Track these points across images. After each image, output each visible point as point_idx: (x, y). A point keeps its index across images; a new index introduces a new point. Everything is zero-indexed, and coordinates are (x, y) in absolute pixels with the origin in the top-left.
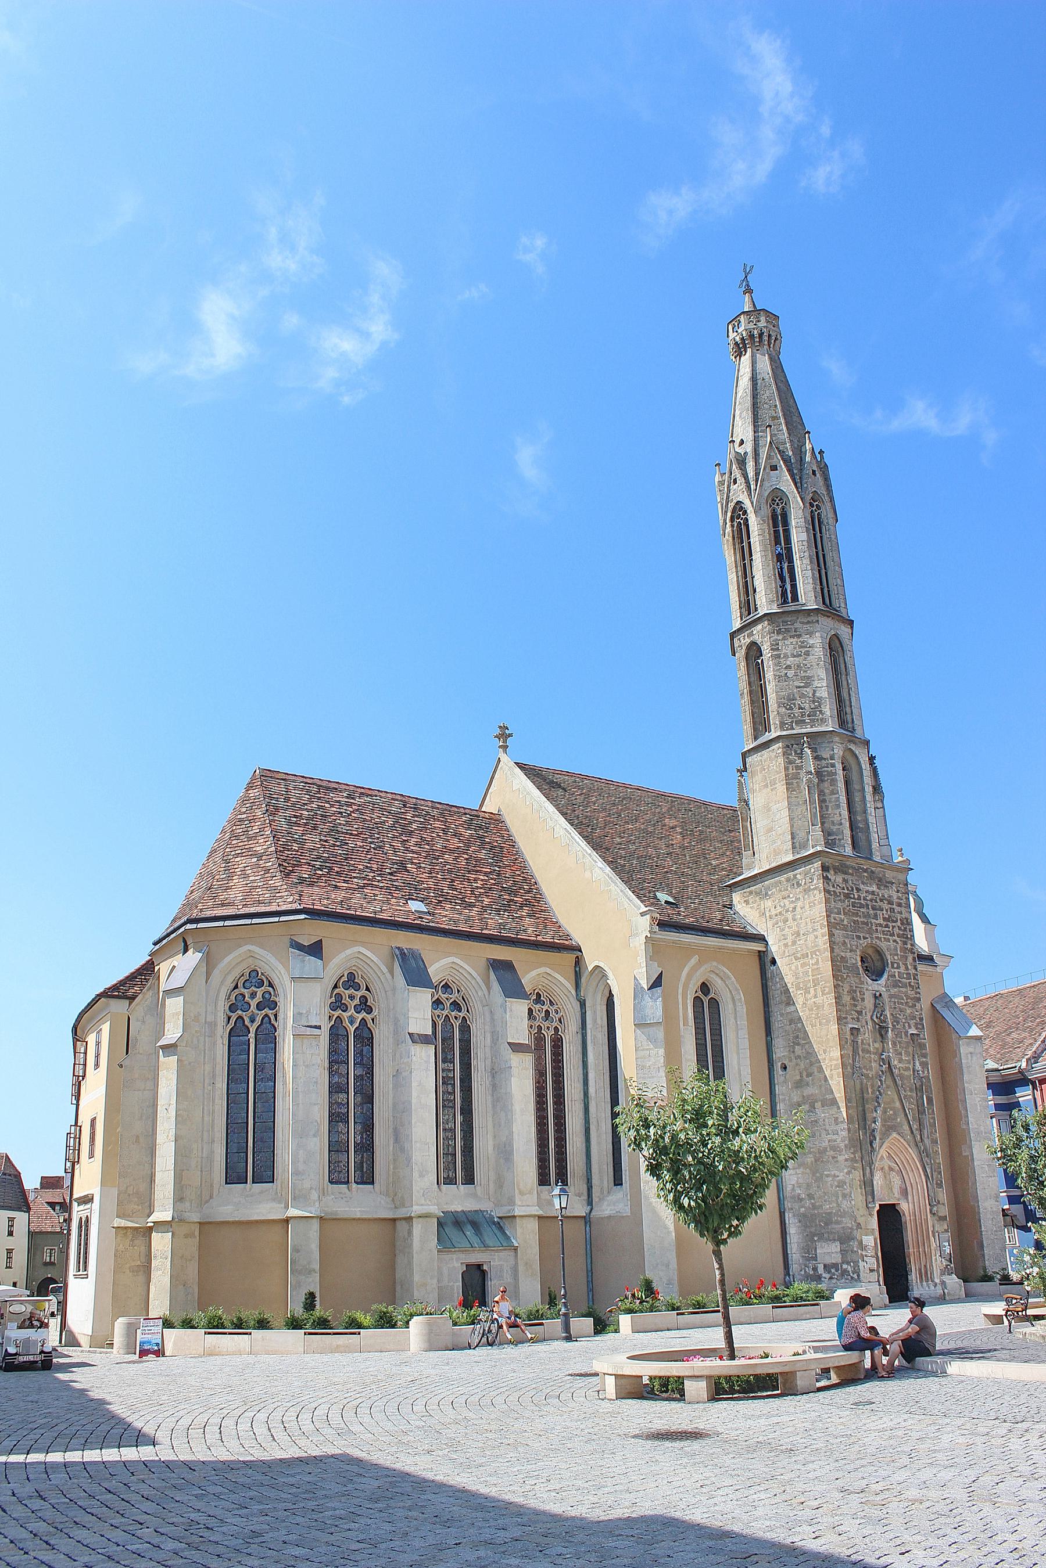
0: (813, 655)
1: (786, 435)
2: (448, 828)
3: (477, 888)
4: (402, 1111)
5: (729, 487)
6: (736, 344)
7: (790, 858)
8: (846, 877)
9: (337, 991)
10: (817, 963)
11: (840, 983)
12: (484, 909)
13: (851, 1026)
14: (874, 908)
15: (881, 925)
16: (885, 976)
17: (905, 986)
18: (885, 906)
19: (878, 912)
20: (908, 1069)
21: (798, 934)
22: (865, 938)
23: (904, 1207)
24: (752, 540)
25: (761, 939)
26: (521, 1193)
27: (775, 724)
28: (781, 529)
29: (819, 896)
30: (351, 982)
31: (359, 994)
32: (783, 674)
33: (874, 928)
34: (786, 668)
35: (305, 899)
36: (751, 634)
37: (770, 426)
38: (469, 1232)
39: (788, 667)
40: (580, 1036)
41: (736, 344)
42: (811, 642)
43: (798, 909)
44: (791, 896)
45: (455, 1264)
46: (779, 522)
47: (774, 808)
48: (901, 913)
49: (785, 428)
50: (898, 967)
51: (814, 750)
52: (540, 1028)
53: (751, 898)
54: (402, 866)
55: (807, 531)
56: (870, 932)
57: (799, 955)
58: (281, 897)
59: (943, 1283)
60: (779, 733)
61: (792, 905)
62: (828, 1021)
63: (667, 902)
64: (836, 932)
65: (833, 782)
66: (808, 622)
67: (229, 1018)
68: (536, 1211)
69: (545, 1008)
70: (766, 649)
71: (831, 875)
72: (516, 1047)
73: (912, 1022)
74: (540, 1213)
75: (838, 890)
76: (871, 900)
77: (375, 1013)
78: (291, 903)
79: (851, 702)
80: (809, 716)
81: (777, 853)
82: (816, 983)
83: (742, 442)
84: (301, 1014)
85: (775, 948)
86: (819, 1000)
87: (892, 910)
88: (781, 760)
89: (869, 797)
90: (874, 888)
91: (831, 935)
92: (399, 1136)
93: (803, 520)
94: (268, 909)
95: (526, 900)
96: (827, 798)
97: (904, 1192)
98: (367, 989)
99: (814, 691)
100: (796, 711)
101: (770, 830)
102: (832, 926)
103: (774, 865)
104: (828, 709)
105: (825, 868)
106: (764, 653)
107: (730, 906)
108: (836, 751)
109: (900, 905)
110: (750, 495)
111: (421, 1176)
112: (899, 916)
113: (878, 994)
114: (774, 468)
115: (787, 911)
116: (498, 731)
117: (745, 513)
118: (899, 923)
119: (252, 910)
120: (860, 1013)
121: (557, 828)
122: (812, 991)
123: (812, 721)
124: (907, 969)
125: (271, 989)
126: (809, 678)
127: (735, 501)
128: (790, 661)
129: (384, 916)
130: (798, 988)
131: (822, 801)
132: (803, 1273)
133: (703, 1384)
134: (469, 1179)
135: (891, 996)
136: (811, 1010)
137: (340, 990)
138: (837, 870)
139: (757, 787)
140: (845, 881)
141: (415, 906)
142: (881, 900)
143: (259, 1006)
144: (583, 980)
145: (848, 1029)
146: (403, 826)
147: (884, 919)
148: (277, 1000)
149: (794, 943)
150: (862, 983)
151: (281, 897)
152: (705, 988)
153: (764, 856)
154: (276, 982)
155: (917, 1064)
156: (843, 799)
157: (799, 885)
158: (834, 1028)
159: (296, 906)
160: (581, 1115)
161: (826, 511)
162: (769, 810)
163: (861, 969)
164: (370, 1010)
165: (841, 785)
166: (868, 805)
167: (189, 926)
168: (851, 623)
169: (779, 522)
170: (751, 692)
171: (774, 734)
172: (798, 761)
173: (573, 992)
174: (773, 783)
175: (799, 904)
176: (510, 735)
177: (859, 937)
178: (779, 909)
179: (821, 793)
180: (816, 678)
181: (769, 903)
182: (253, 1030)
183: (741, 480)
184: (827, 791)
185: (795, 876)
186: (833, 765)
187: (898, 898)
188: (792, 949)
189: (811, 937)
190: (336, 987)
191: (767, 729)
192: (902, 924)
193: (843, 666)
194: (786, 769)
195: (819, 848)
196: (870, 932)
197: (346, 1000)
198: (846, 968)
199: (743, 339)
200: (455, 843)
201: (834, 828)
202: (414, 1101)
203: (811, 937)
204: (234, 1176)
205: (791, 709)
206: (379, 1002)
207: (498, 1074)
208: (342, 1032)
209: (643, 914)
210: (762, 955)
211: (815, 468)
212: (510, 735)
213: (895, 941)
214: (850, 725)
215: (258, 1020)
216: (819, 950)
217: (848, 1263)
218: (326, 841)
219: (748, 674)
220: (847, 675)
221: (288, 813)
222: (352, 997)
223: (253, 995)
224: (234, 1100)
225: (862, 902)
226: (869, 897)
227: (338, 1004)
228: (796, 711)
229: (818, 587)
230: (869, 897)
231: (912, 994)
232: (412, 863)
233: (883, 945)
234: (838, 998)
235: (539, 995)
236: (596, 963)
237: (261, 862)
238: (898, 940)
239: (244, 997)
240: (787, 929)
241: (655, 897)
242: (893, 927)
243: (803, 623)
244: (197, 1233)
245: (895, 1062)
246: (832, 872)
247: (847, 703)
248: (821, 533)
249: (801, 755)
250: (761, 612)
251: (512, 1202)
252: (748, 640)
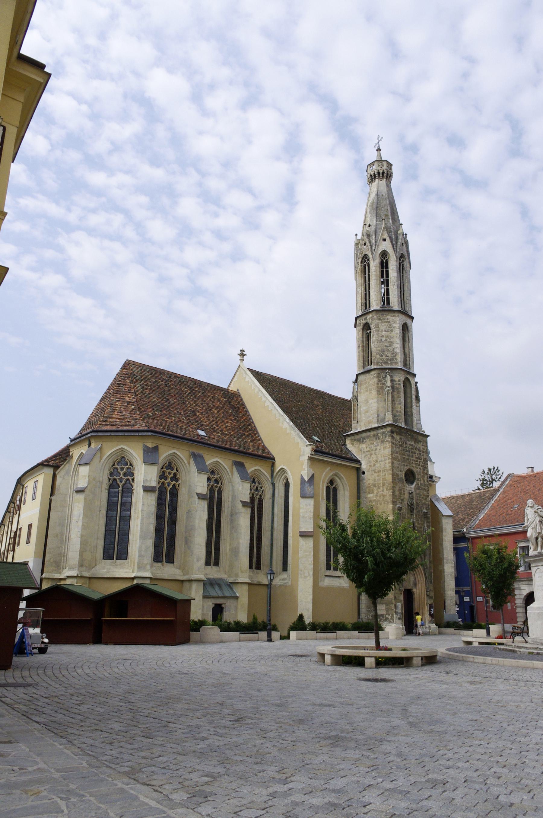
0: (395, 332)
1: (391, 224)
2: (215, 397)
3: (228, 426)
4: (189, 530)
5: (361, 246)
6: (371, 176)
7: (375, 425)
8: (401, 437)
9: (163, 470)
10: (385, 475)
11: (395, 486)
12: (231, 436)
13: (398, 506)
14: (412, 452)
15: (414, 460)
16: (415, 484)
17: (423, 489)
18: (417, 452)
19: (414, 454)
20: (421, 528)
21: (377, 461)
22: (407, 466)
23: (414, 590)
24: (371, 274)
25: (358, 462)
26: (242, 572)
27: (374, 362)
28: (385, 270)
29: (388, 445)
30: (169, 465)
31: (173, 472)
32: (380, 339)
33: (411, 462)
34: (381, 337)
35: (151, 426)
36: (366, 319)
37: (384, 219)
38: (217, 588)
39: (383, 336)
40: (271, 500)
41: (371, 176)
42: (394, 325)
43: (378, 450)
44: (375, 443)
45: (210, 604)
46: (384, 265)
47: (370, 402)
48: (423, 455)
49: (391, 221)
50: (420, 481)
51: (391, 376)
52: (253, 495)
53: (355, 443)
54: (194, 412)
55: (397, 272)
56: (410, 463)
57: (376, 471)
58: (139, 423)
59: (429, 627)
60: (375, 367)
61: (375, 448)
62: (388, 503)
63: (317, 441)
64: (395, 462)
65: (399, 392)
66: (394, 316)
67: (109, 479)
68: (247, 580)
69: (256, 485)
70: (372, 326)
71: (395, 435)
72: (244, 504)
73: (425, 506)
74: (250, 581)
75: (397, 443)
76: (411, 449)
77: (179, 482)
78: (144, 427)
79: (409, 356)
80: (390, 360)
81: (369, 422)
82: (384, 485)
83: (370, 226)
84: (146, 480)
85: (364, 466)
86: (385, 493)
87: (420, 454)
88: (376, 380)
89: (414, 401)
90: (413, 443)
91: (393, 463)
92: (187, 541)
93: (395, 267)
94: (133, 429)
95: (250, 434)
96: (395, 399)
97: (415, 584)
98: (177, 470)
99: (394, 349)
100: (384, 357)
101: (367, 412)
102: (393, 459)
103: (368, 428)
104: (399, 358)
105: (392, 432)
106: (372, 328)
107: (345, 445)
108: (401, 378)
109: (423, 452)
110: (372, 252)
111: (198, 561)
112: (422, 457)
113: (411, 492)
114: (384, 240)
115: (372, 450)
116: (239, 352)
117: (368, 260)
118: (422, 460)
119: (125, 428)
120: (402, 500)
121: (267, 401)
122: (381, 488)
123: (391, 363)
124: (424, 481)
125: (131, 467)
126: (392, 342)
127: (364, 254)
128: (384, 333)
129: (187, 436)
130: (375, 486)
131: (393, 401)
132: (366, 618)
133: (373, 660)
134: (217, 564)
135: (416, 494)
136: (380, 497)
137: (174, 471)
138: (398, 433)
139: (362, 391)
140: (401, 439)
141: (201, 433)
142: (415, 449)
143: (125, 474)
144: (275, 474)
145: (397, 507)
146: (194, 394)
147: (416, 458)
148: (134, 472)
149: (374, 465)
150: (404, 486)
151: (139, 423)
152: (331, 482)
153: (363, 423)
154: (134, 464)
155: (426, 526)
156: (403, 400)
157: (379, 439)
158: (391, 506)
159: (146, 428)
160: (270, 537)
161: (406, 263)
162: (367, 402)
163: (404, 481)
165: (402, 394)
166: (413, 404)
167: (93, 434)
168: (412, 318)
169: (384, 265)
170: (363, 346)
171: (373, 367)
172: (383, 381)
173: (270, 479)
174: (371, 390)
175: (379, 447)
176: (245, 355)
177: (404, 465)
178: (368, 449)
179: (393, 397)
180: (395, 343)
181: (363, 446)
182: (121, 485)
183: (369, 244)
184: (395, 396)
185: (377, 434)
186: (399, 384)
187: (423, 449)
188: (373, 468)
189: (383, 463)
190: (162, 468)
191: (369, 363)
192: (424, 461)
193: (407, 338)
194: (378, 384)
195: (390, 422)
196: (410, 463)
197: (167, 474)
198: (398, 479)
199: (374, 174)
200: (218, 404)
201: (398, 414)
202: (197, 525)
203: (383, 463)
204: (108, 555)
205: (382, 356)
206: (182, 476)
207: (233, 514)
208: (164, 490)
209: (307, 445)
210: (358, 469)
211: (403, 242)
212: (245, 355)
213: (420, 468)
214: (408, 366)
215: (124, 481)
216: (386, 470)
217: (389, 615)
218: (159, 398)
219: (363, 338)
220: (409, 343)
221: (142, 383)
222: (169, 473)
223: (122, 469)
224: (109, 520)
225: (407, 449)
226: (410, 447)
227: (162, 476)
228: (384, 357)
229: (400, 300)
230: (410, 447)
231: (425, 493)
232: (199, 412)
233: (415, 470)
234: (394, 492)
235: (254, 479)
236: (282, 467)
237: (129, 406)
238: (421, 468)
239: (118, 470)
240: (371, 459)
241: (312, 438)
242: (420, 462)
243: (392, 316)
244: (88, 582)
245: (416, 524)
246: (395, 434)
247: (408, 356)
248: (403, 274)
249: (385, 378)
250: (372, 309)
251: (237, 575)
252: (364, 322)
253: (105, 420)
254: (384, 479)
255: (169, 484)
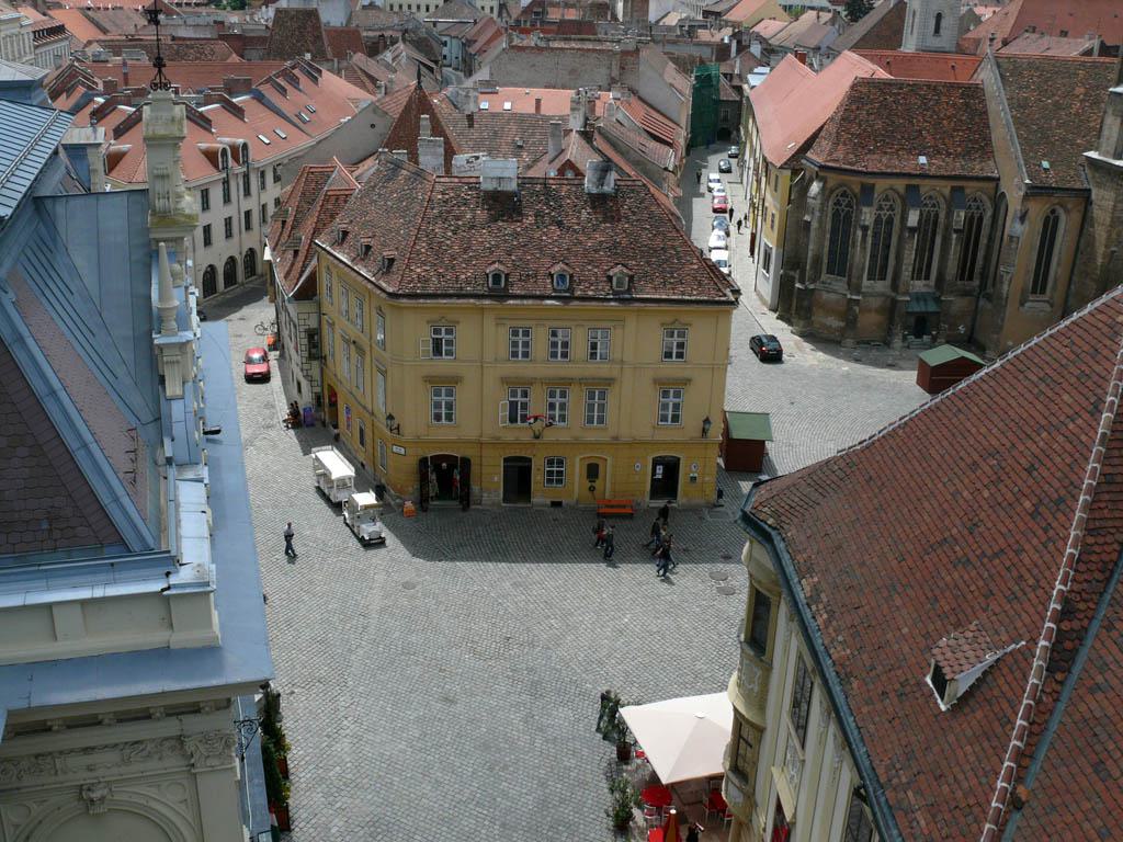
38: (922, 303)
54: (920, 131)
85: (1093, 197)
129: (906, 170)
141: (923, 160)
164: (893, 210)
181: (1097, 175)
200: (951, 111)
234: (1109, 237)
253: (830, 154)
254: (1104, 220)
255: (885, 214)
